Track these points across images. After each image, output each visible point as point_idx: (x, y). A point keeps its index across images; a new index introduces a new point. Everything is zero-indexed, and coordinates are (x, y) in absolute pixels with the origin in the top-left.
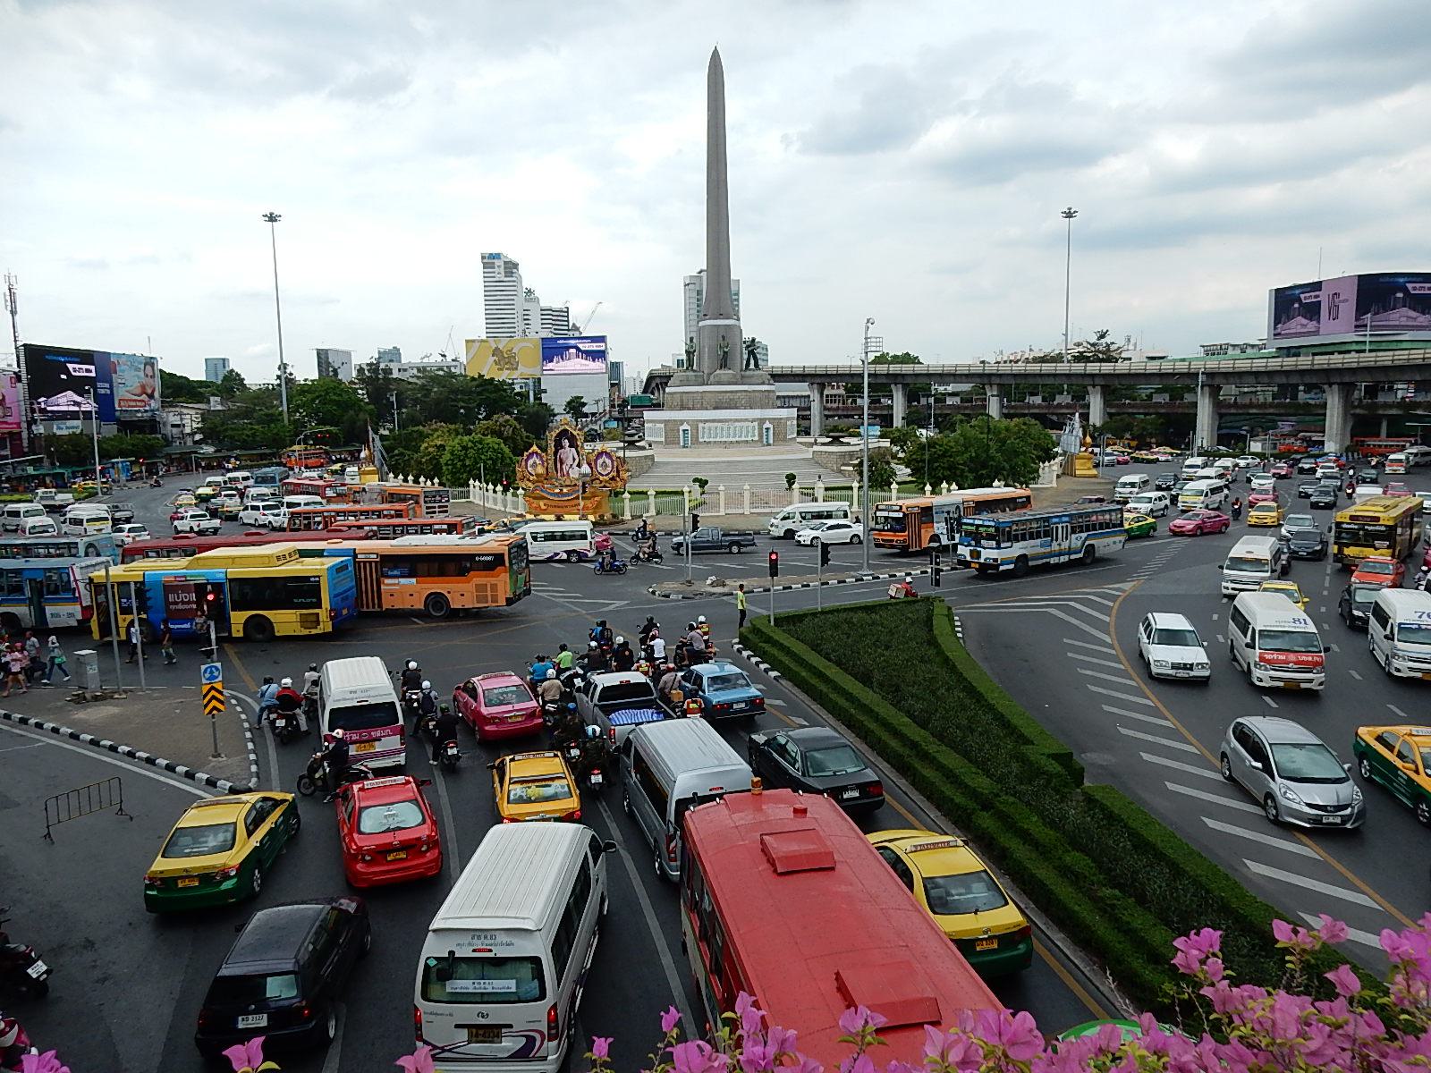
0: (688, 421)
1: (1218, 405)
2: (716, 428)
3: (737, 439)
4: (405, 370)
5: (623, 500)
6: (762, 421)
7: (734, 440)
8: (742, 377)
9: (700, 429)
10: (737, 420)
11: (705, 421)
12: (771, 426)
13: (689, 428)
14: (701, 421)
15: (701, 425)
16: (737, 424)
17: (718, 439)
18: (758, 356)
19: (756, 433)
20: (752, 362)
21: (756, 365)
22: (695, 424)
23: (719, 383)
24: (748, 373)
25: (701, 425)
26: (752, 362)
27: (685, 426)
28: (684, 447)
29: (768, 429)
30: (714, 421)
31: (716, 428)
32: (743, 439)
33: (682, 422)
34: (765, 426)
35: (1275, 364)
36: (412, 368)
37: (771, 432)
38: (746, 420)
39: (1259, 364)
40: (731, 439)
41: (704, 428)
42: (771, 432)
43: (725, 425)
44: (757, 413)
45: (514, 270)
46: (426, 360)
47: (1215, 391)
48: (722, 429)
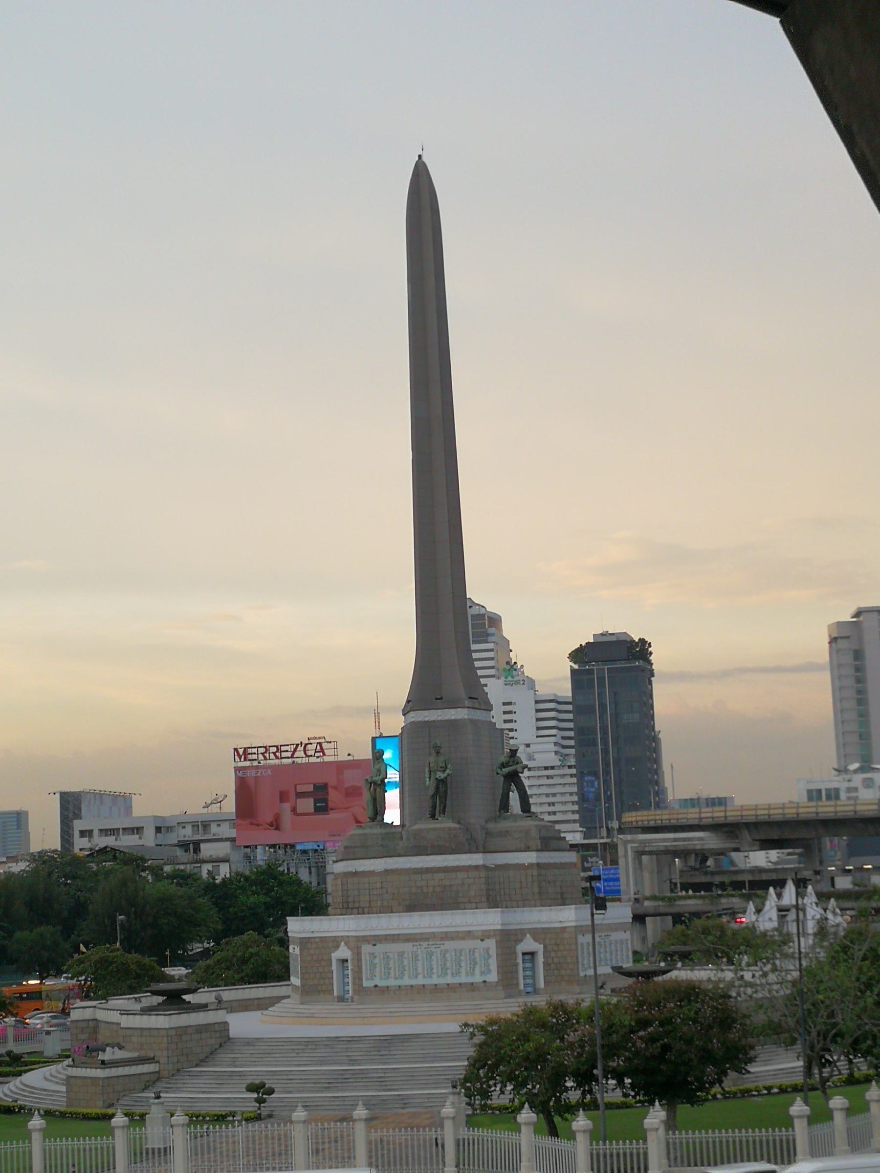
0: (347, 940)
2: (401, 954)
3: (449, 980)
4: (169, 829)
5: (111, 1132)
6: (507, 939)
7: (442, 981)
8: (488, 834)
9: (365, 958)
10: (447, 936)
11: (376, 940)
13: (539, 948)
14: (366, 939)
15: (366, 949)
16: (449, 945)
17: (406, 981)
18: (526, 783)
19: (493, 963)
20: (514, 797)
21: (526, 806)
22: (357, 943)
24: (503, 825)
25: (366, 949)
26: (514, 797)
27: (344, 952)
28: (341, 999)
29: (532, 954)
32: (464, 979)
33: (335, 942)
34: (522, 947)
36: (182, 825)
37: (540, 959)
38: (468, 935)
40: (435, 980)
41: (373, 955)
42: (540, 959)
43: (421, 949)
44: (491, 919)
45: (492, 630)
46: (215, 808)
48: (415, 957)
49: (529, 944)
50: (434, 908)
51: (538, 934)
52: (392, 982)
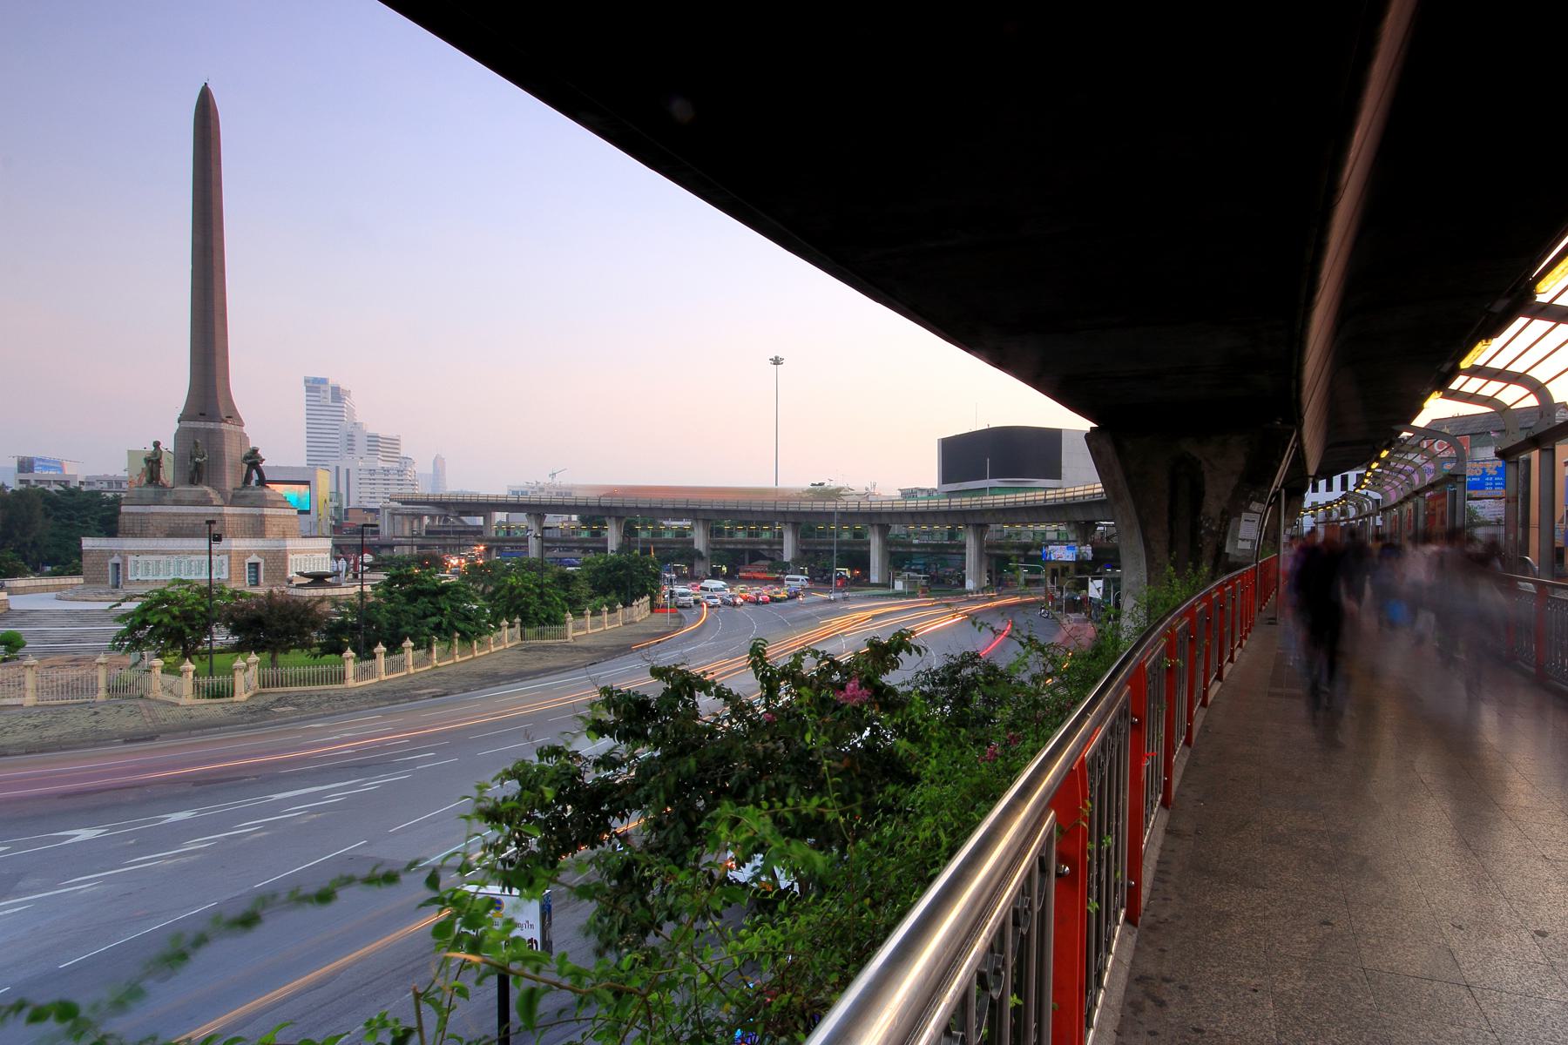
1: (886, 543)
2: (158, 562)
11: (139, 553)
12: (262, 561)
14: (132, 553)
16: (193, 557)
19: (225, 569)
22: (124, 554)
23: (177, 503)
25: (131, 558)
27: (116, 559)
29: (257, 565)
30: (153, 553)
31: (158, 562)
33: (112, 553)
35: (944, 503)
37: (262, 567)
39: (933, 503)
43: (173, 559)
47: (884, 529)
49: (254, 559)
50: (187, 536)
51: (259, 553)
52: (150, 578)
